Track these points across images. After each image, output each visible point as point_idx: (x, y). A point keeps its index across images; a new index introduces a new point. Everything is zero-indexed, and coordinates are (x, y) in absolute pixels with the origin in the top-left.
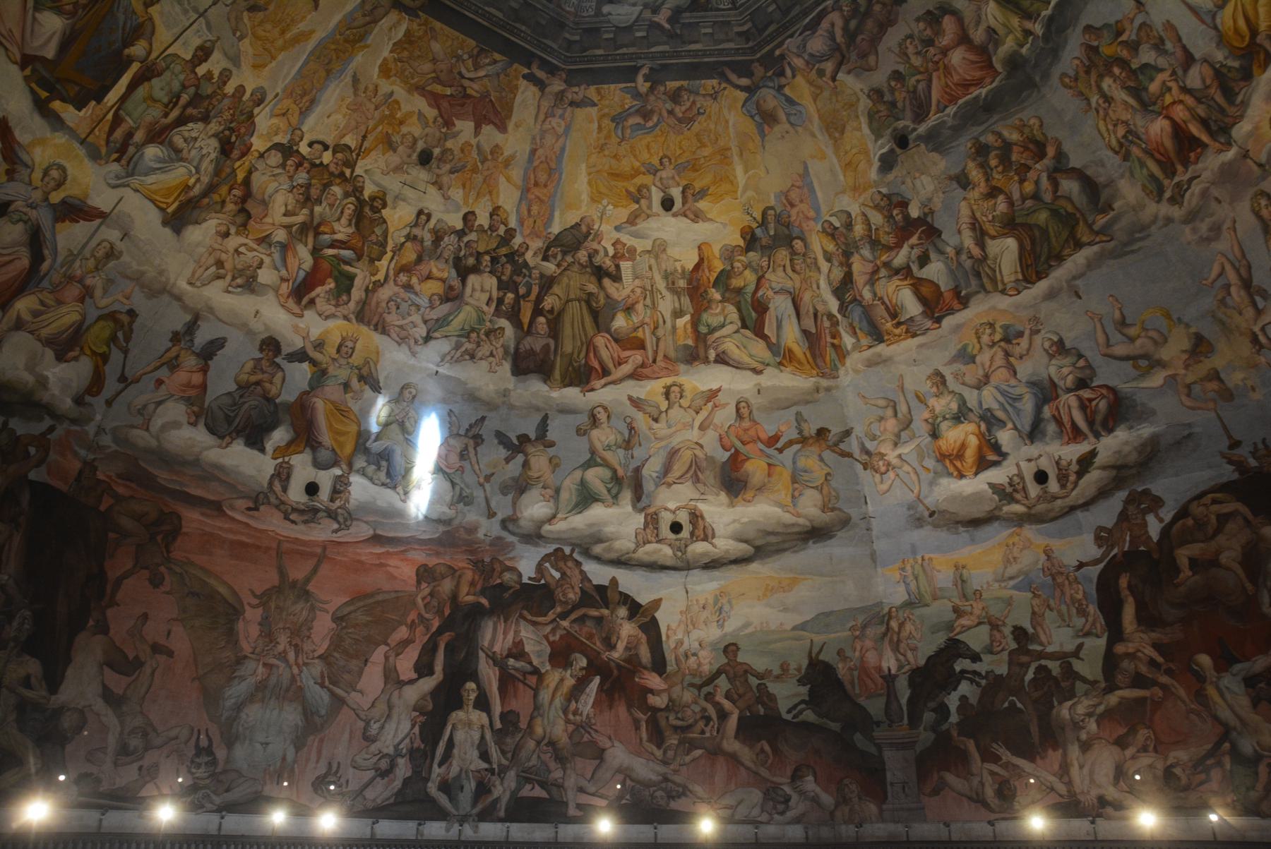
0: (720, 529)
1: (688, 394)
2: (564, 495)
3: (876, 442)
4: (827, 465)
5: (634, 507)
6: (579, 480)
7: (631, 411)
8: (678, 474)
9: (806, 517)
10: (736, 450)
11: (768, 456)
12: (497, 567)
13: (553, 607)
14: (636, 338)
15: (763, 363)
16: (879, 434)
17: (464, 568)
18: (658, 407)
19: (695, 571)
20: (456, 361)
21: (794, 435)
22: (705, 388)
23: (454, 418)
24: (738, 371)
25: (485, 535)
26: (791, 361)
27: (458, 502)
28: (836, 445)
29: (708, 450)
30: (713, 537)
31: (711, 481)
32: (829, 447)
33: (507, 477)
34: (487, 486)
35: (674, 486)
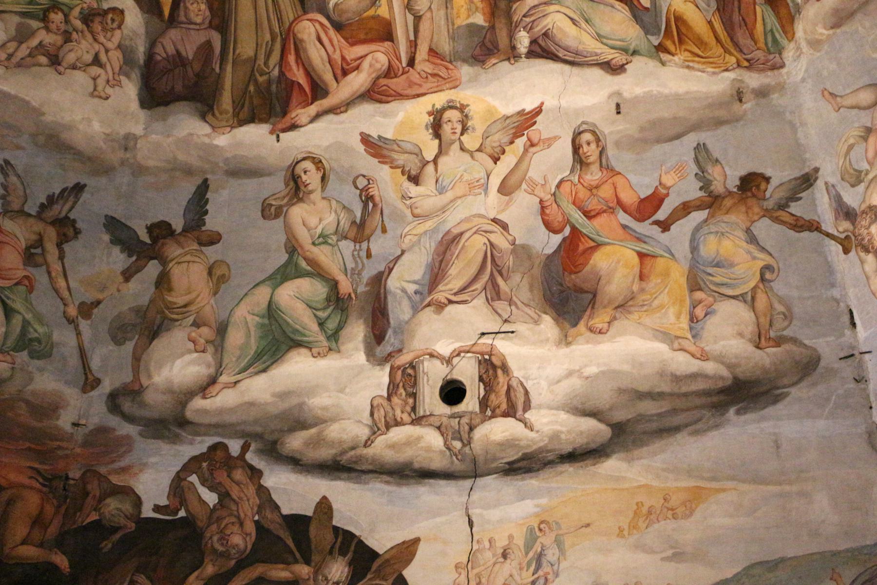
0: (540, 392)
1: (478, 124)
2: (235, 338)
3: (861, 187)
4: (763, 249)
5: (370, 354)
6: (264, 305)
7: (368, 164)
8: (457, 284)
9: (720, 359)
10: (575, 230)
11: (640, 239)
12: (94, 488)
13: (197, 565)
14: (376, 18)
15: (625, 50)
16: (865, 166)
17: (23, 486)
18: (419, 153)
19: (489, 480)
20: (19, 65)
21: (692, 191)
22: (510, 109)
23: (13, 179)
24: (575, 70)
25: (75, 425)
26: (681, 42)
27: (17, 348)
28: (782, 206)
29: (518, 233)
30: (527, 406)
31: (524, 294)
32: (767, 213)
33: (125, 308)
34: (84, 324)
35: (450, 308)
